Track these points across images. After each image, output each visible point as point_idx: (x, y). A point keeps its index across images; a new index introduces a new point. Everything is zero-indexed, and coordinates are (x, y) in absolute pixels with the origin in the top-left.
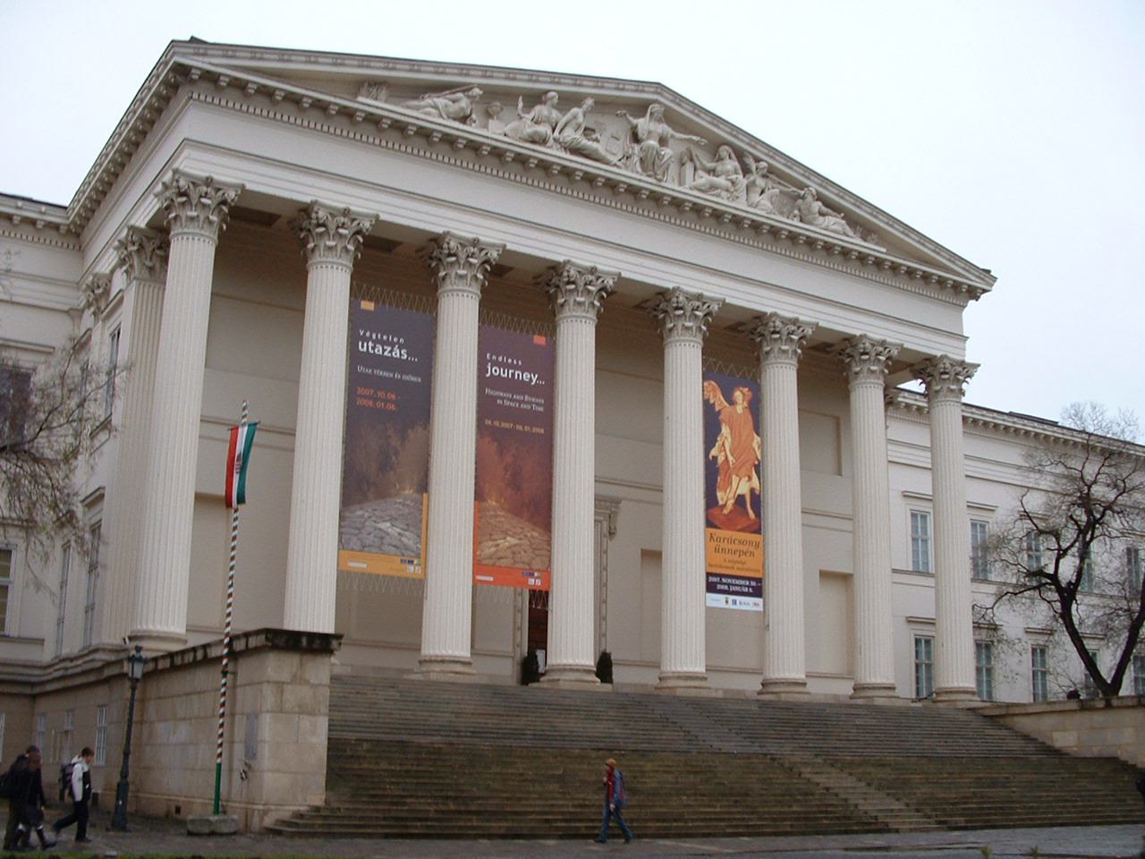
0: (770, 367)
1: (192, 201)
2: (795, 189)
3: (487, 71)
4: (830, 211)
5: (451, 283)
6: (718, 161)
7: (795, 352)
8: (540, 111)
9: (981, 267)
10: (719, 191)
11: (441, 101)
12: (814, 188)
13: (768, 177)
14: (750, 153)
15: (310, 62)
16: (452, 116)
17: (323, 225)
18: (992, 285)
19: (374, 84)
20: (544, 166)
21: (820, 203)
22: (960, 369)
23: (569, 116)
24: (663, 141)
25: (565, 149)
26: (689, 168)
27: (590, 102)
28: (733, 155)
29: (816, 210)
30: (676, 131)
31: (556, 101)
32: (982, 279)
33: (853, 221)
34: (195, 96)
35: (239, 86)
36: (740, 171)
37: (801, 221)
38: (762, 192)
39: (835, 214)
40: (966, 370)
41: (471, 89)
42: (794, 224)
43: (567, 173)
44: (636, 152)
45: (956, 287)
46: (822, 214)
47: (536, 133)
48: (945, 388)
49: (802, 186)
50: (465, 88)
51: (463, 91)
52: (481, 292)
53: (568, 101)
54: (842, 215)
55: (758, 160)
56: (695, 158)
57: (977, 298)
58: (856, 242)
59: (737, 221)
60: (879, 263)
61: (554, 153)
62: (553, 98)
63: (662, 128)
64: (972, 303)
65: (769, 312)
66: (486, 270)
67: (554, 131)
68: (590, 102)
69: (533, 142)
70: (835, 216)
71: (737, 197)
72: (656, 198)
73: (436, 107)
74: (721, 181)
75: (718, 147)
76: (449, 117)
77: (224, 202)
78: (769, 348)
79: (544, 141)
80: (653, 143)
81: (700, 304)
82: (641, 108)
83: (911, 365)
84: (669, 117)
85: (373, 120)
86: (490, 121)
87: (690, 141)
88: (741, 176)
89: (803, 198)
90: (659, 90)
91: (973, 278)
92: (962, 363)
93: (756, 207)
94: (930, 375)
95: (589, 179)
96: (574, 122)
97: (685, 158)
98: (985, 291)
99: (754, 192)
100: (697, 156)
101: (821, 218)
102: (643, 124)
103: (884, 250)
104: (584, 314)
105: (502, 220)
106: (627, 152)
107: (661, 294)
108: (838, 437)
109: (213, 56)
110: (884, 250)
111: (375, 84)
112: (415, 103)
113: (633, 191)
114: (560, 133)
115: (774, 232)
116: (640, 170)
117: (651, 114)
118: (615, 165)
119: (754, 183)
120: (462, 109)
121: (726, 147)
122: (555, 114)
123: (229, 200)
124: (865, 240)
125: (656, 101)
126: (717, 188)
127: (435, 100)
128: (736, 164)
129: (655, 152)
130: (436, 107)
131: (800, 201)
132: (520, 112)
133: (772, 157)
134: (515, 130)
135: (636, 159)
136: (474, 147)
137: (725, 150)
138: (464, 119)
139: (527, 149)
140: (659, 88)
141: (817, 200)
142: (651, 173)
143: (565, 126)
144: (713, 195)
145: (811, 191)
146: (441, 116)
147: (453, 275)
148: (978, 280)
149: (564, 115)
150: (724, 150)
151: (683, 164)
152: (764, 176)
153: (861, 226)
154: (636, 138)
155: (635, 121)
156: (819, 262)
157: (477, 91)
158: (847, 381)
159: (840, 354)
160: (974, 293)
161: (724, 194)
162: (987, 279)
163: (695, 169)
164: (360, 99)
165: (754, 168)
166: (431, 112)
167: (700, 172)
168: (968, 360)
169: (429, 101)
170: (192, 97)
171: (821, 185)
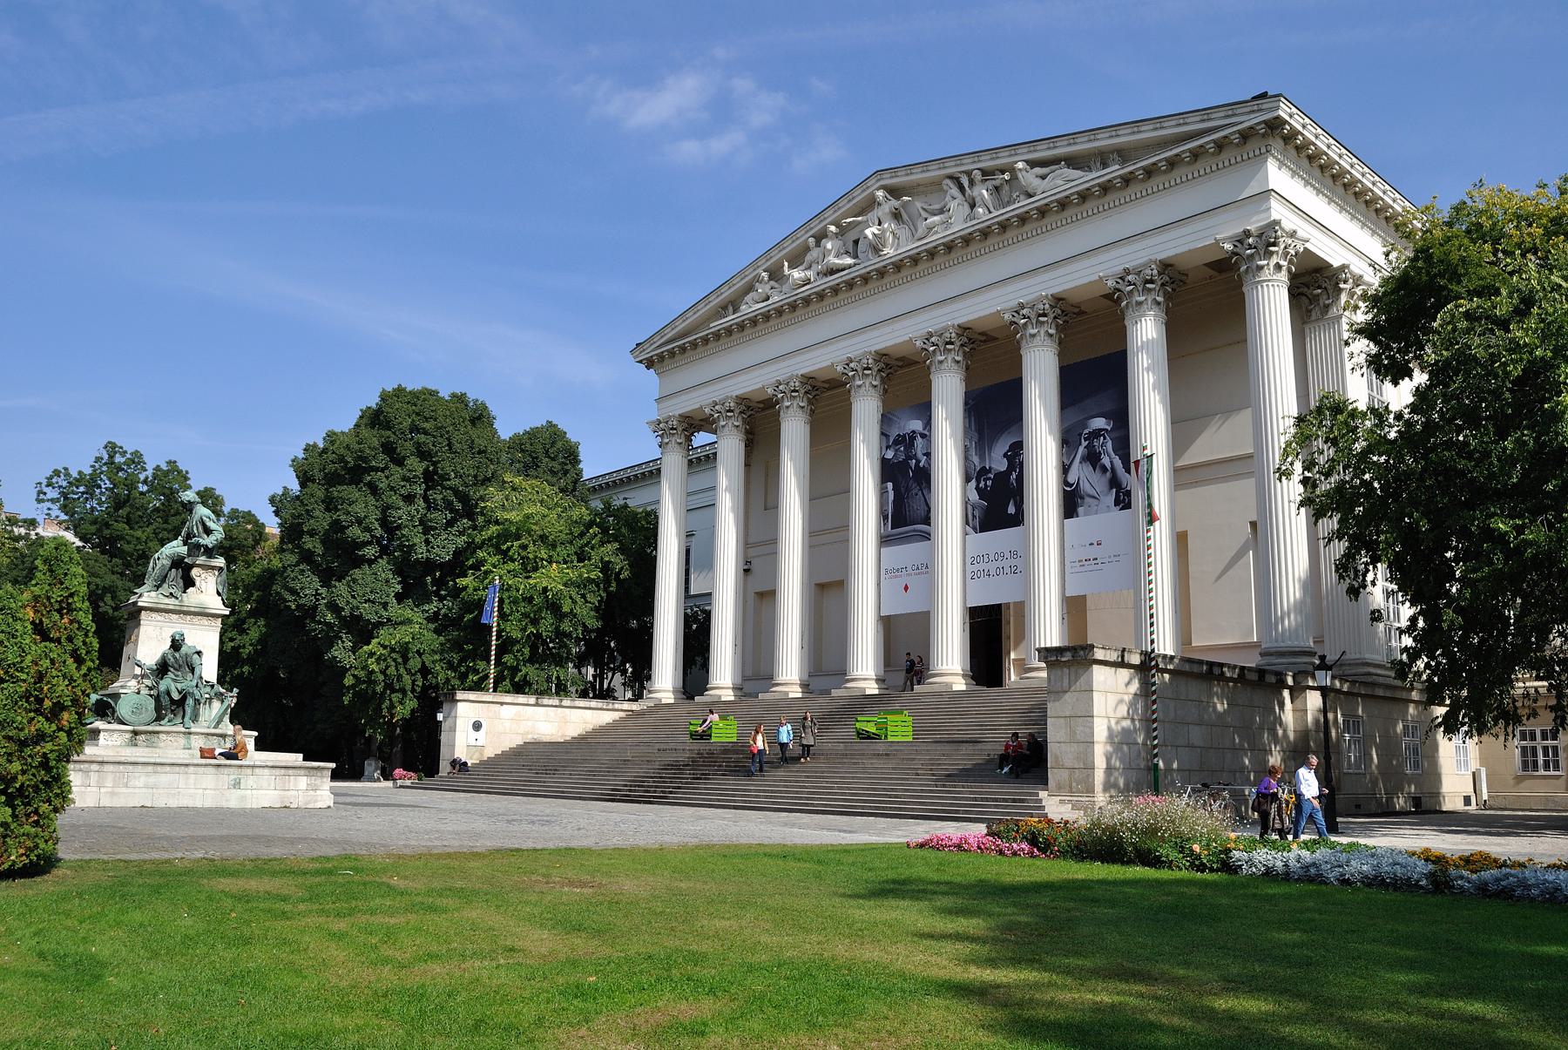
4: (1053, 167)
11: (748, 298)
13: (986, 180)
14: (960, 172)
21: (1038, 170)
24: (896, 216)
25: (825, 275)
32: (1259, 110)
33: (1073, 162)
42: (1022, 205)
46: (1043, 177)
54: (1063, 163)
55: (969, 173)
59: (949, 247)
78: (861, 382)
89: (1014, 177)
90: (879, 177)
108: (767, 475)
109: (647, 348)
110: (1117, 167)
128: (955, 191)
138: (768, 299)
144: (932, 235)
148: (1252, 116)
150: (945, 187)
164: (711, 325)
165: (966, 183)
166: (750, 308)
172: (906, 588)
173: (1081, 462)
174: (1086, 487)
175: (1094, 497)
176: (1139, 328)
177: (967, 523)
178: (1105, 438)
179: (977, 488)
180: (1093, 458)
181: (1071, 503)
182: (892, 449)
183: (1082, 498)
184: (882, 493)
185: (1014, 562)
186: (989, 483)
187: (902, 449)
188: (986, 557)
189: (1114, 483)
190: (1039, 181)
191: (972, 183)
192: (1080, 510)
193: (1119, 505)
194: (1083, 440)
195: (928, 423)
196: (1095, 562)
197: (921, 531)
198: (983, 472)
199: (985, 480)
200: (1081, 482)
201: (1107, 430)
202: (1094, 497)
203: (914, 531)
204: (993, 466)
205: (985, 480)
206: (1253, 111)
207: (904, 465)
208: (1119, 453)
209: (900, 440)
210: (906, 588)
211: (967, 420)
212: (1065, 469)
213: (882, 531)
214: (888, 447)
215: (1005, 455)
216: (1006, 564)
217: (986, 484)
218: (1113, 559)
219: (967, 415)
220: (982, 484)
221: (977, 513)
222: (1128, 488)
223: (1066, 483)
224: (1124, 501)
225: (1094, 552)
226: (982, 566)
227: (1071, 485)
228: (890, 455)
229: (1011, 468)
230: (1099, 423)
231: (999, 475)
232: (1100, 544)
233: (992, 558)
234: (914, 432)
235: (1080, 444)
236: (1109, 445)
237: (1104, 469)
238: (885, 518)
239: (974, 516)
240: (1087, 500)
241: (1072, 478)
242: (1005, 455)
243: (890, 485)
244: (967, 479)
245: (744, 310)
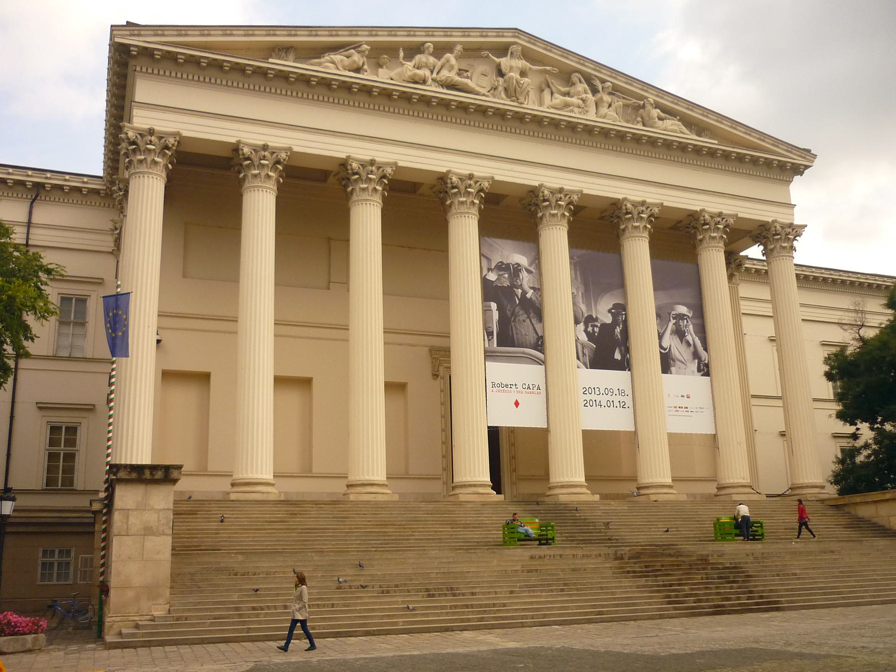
0: (627, 240)
1: (141, 147)
2: (636, 101)
3: (372, 30)
5: (357, 195)
6: (571, 86)
7: (645, 227)
8: (420, 59)
9: (802, 147)
10: (571, 108)
11: (337, 57)
12: (652, 98)
13: (614, 94)
15: (227, 35)
16: (347, 68)
17: (356, 173)
19: (283, 50)
20: (425, 101)
21: (658, 110)
22: (719, 219)
23: (443, 60)
24: (523, 74)
25: (442, 86)
26: (547, 94)
27: (459, 48)
28: (582, 79)
29: (656, 115)
30: (533, 65)
31: (431, 50)
33: (689, 123)
34: (138, 69)
35: (171, 57)
36: (589, 91)
37: (644, 125)
38: (610, 106)
39: (672, 117)
40: (796, 231)
41: (360, 46)
42: (638, 128)
43: (445, 104)
44: (501, 83)
45: (782, 166)
46: (660, 119)
47: (415, 75)
48: (778, 246)
49: (642, 98)
50: (356, 46)
51: (354, 48)
52: (382, 201)
53: (441, 50)
54: (678, 117)
55: (603, 81)
56: (550, 84)
57: (801, 174)
58: (691, 138)
60: (712, 153)
61: (432, 90)
62: (428, 48)
63: (522, 63)
64: (797, 178)
65: (699, 210)
66: (482, 197)
67: (432, 72)
68: (459, 48)
69: (416, 82)
70: (673, 119)
71: (587, 111)
72: (520, 118)
73: (333, 62)
74: (574, 100)
75: (571, 74)
76: (345, 69)
77: (167, 147)
79: (424, 82)
80: (515, 75)
81: (562, 195)
82: (503, 50)
83: (750, 232)
84: (526, 55)
85: (283, 76)
86: (380, 70)
87: (546, 72)
88: (590, 96)
89: (644, 107)
90: (517, 34)
91: (795, 157)
92: (791, 225)
93: (604, 118)
94: (765, 238)
95: (463, 107)
96: (447, 65)
97: (544, 86)
98: (807, 167)
99: (603, 107)
100: (552, 83)
101: (660, 122)
102: (504, 62)
103: (716, 142)
104: (467, 211)
105: (279, 127)
106: (494, 85)
107: (532, 191)
110: (716, 142)
111: (283, 49)
112: (317, 60)
113: (501, 114)
114: (438, 73)
115: (621, 136)
116: (503, 96)
117: (512, 53)
118: (484, 95)
119: (601, 99)
120: (355, 61)
121: (577, 74)
122: (432, 60)
123: (282, 160)
124: (700, 136)
125: (515, 43)
126: (570, 106)
127: (332, 56)
129: (514, 81)
130: (333, 62)
131: (641, 111)
132: (401, 60)
133: (615, 78)
134: (400, 75)
135: (501, 88)
136: (366, 90)
137: (577, 77)
138: (358, 70)
139: (409, 88)
140: (517, 32)
141: (655, 108)
142: (514, 98)
143: (442, 67)
144: (567, 111)
145: (649, 101)
146: (338, 69)
147: (358, 189)
149: (439, 60)
150: (575, 77)
151: (542, 91)
152: (610, 94)
153: (695, 126)
154: (501, 73)
155: (497, 60)
156: (710, 166)
157: (365, 47)
158: (694, 247)
159: (687, 227)
160: (798, 170)
161: (576, 110)
162: (807, 157)
163: (552, 93)
164: (271, 60)
165: (600, 88)
167: (556, 95)
168: (797, 222)
169: (327, 58)
170: (135, 70)
171: (657, 96)
172: (517, 404)
173: (671, 334)
174: (675, 353)
175: (683, 362)
176: (257, 198)
177: (578, 358)
178: (687, 322)
179: (586, 331)
180: (680, 333)
181: (667, 363)
182: (494, 272)
183: (674, 361)
184: (486, 311)
185: (622, 399)
186: (596, 330)
187: (506, 276)
188: (597, 390)
189: (696, 355)
190: (657, 119)
191: (603, 88)
192: (673, 369)
193: (700, 372)
194: (672, 319)
195: (537, 260)
196: (686, 410)
197: (531, 355)
198: (590, 320)
199: (593, 326)
200: (672, 349)
201: (689, 317)
202: (683, 362)
203: (524, 353)
204: (599, 317)
205: (593, 326)
206: (800, 156)
207: (509, 292)
208: (697, 335)
209: (502, 267)
210: (517, 404)
211: (573, 272)
212: (661, 337)
213: (487, 345)
214: (489, 270)
215: (610, 311)
216: (616, 399)
217: (593, 330)
218: (698, 410)
219: (573, 268)
220: (590, 329)
221: (586, 351)
222: (706, 362)
223: (661, 347)
224: (705, 370)
225: (684, 402)
226: (593, 397)
227: (665, 349)
228: (492, 277)
229: (615, 323)
230: (682, 309)
231: (604, 325)
232: (689, 397)
233: (602, 391)
234: (519, 265)
235: (670, 321)
236: (691, 327)
237: (688, 344)
238: (490, 334)
239: (584, 354)
240: (678, 363)
241: (665, 344)
242: (610, 311)
243: (494, 306)
244: (577, 322)
245: (327, 67)
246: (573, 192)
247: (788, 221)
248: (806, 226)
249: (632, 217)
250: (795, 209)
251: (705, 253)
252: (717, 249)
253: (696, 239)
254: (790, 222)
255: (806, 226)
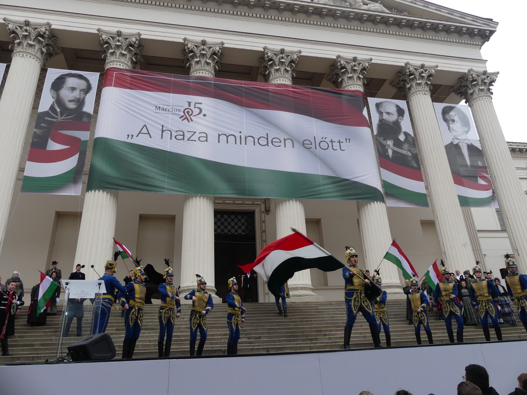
18: (496, 28)
32: (487, 25)
162: (491, 24)
206: (485, 24)
246: (293, 53)
247: (481, 70)
248: (498, 73)
249: (347, 70)
250: (487, 62)
251: (414, 97)
252: (424, 92)
253: (406, 88)
254: (483, 70)
255: (498, 73)
